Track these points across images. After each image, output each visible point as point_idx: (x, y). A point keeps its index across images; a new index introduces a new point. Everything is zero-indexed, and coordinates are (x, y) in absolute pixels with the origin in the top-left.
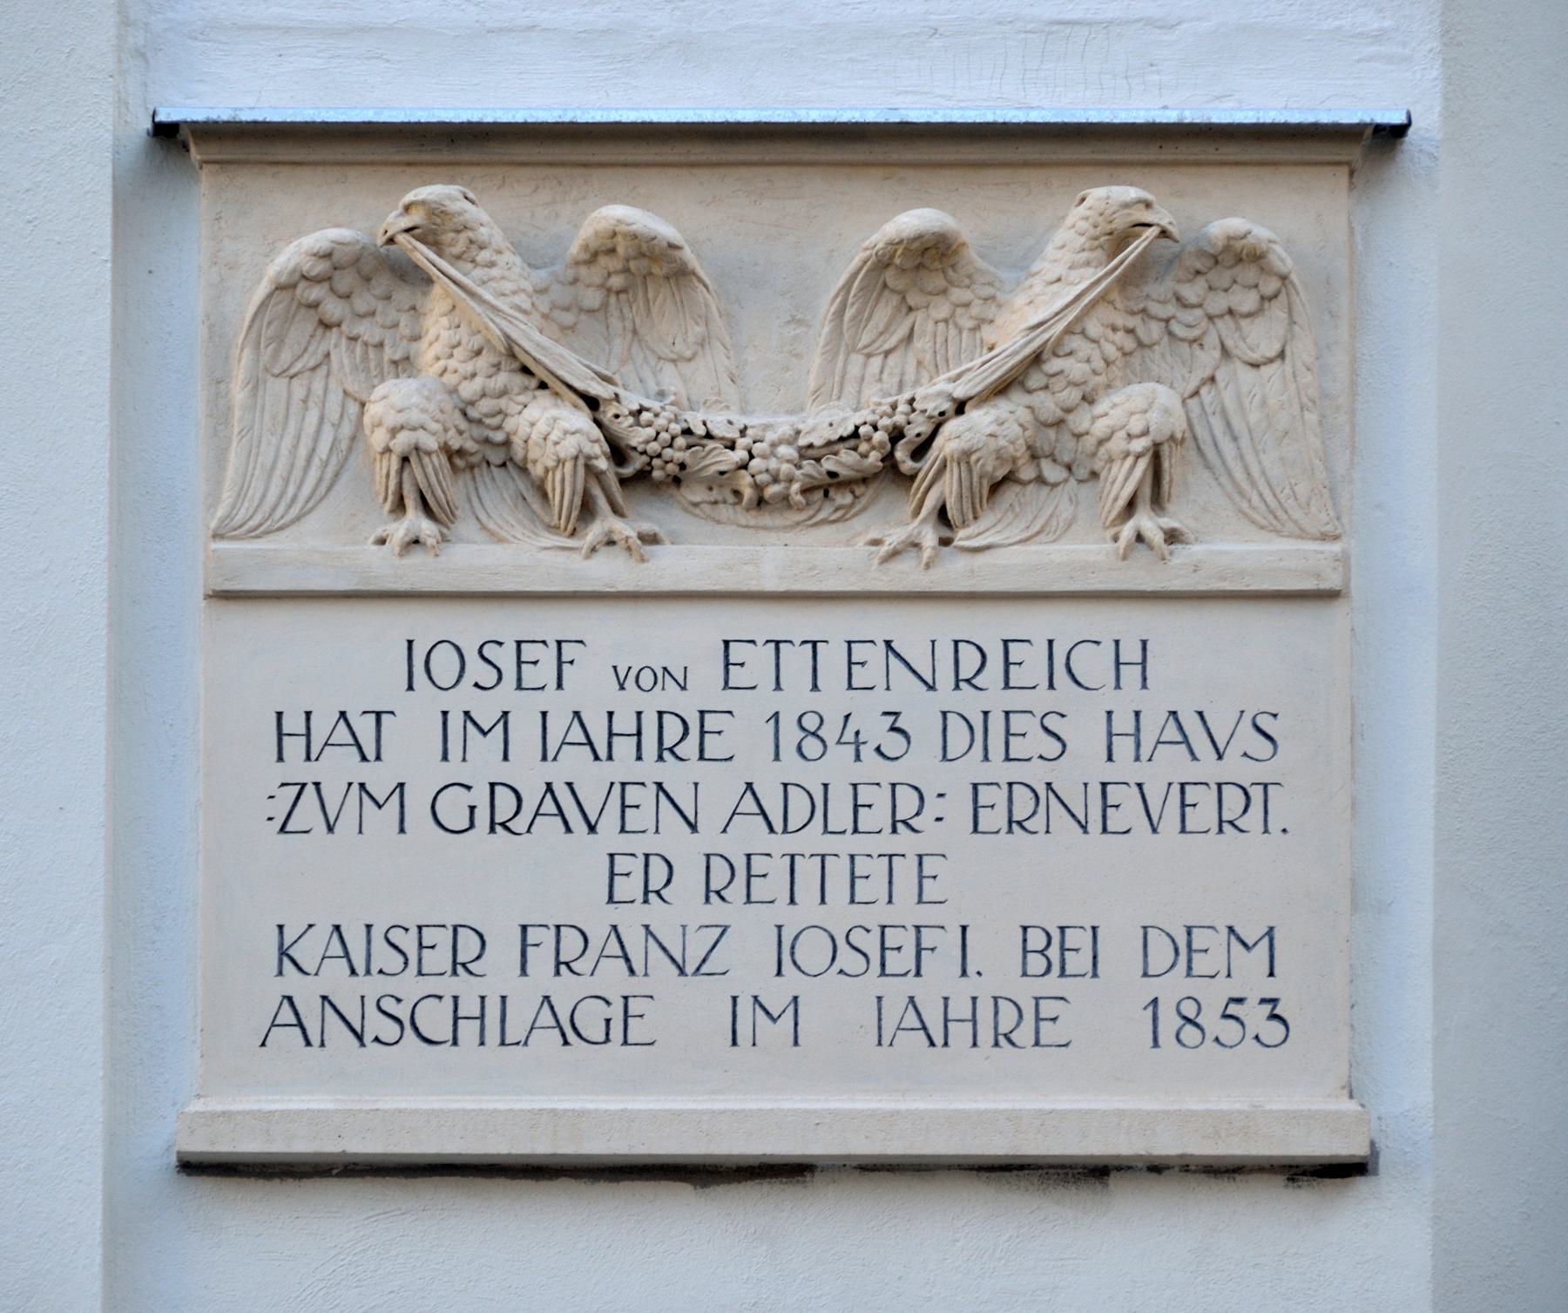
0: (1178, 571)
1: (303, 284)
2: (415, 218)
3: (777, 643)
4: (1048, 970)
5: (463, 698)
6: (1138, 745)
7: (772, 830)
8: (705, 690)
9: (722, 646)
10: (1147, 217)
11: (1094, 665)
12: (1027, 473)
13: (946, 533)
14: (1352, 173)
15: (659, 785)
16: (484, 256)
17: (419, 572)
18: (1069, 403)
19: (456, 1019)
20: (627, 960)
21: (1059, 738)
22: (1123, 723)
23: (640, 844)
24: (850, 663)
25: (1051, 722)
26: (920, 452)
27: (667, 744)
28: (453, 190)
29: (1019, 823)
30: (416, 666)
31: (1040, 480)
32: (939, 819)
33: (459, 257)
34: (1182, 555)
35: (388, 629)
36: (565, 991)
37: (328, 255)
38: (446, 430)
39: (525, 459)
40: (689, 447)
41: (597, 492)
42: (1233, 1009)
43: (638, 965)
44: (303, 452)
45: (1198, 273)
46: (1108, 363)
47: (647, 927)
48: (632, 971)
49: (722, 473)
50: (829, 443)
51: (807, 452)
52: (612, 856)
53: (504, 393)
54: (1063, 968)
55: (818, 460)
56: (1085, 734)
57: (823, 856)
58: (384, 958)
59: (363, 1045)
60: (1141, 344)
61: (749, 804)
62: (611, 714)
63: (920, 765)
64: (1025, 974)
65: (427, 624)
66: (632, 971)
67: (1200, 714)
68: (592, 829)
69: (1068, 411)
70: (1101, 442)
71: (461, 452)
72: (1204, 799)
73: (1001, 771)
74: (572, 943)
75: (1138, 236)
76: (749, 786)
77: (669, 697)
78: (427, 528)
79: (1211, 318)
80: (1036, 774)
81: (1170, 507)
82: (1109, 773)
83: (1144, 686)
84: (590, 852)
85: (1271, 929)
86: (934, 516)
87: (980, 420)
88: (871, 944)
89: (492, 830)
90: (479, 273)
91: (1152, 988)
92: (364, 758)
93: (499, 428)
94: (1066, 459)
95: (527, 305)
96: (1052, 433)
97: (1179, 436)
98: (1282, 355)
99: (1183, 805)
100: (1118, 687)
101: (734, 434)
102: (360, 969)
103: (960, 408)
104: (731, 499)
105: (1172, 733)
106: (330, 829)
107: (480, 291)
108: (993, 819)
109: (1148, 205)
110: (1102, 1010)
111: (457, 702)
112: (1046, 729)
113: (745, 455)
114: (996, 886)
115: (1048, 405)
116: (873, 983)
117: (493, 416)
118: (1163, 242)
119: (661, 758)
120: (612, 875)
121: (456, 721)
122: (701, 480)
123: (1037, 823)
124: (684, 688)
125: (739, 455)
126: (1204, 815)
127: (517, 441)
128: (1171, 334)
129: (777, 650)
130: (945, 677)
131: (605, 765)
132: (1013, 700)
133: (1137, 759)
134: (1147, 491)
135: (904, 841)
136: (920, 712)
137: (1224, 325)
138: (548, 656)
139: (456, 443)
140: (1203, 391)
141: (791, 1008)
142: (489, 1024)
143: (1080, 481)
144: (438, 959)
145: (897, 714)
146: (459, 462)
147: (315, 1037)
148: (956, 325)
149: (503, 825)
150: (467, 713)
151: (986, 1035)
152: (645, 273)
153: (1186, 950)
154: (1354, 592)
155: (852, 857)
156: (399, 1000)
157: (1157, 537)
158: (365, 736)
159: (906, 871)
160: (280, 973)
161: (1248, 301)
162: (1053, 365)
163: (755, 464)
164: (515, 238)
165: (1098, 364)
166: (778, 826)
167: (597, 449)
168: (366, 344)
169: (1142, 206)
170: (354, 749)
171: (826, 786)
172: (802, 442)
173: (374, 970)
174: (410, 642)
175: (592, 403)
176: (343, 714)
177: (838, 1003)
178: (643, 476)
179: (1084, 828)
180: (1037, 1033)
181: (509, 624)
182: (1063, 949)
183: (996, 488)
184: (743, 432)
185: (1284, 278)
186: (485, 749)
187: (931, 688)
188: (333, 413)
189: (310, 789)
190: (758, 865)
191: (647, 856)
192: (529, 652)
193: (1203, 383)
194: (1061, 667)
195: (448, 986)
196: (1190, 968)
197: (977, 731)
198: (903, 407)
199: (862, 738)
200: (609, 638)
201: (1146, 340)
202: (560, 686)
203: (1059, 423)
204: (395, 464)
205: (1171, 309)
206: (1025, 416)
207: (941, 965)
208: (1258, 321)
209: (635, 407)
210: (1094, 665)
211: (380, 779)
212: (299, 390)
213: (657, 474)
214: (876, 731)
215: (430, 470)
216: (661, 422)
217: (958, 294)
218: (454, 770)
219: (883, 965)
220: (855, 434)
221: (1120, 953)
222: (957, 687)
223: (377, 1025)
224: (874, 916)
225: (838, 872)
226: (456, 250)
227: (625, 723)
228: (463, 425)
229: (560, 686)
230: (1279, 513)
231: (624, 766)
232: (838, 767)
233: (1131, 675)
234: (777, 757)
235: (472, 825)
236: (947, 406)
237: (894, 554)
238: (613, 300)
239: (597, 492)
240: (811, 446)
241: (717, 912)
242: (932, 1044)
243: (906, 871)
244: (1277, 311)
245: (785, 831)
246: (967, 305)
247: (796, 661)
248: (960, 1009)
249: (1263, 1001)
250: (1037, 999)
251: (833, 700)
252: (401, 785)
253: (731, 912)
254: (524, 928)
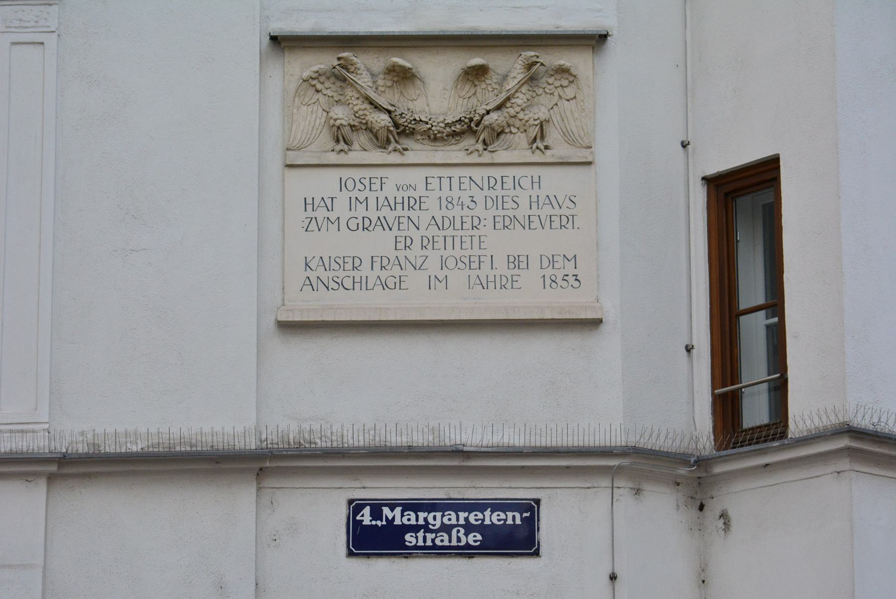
0: (549, 157)
5: (355, 193)
8: (421, 190)
10: (538, 60)
11: (526, 183)
12: (507, 130)
16: (359, 72)
22: (534, 199)
23: (404, 234)
26: (477, 125)
28: (351, 54)
30: (343, 185)
31: (511, 132)
36: (384, 275)
37: (317, 72)
41: (391, 137)
42: (565, 278)
43: (403, 267)
51: (447, 125)
56: (524, 202)
58: (334, 266)
61: (433, 222)
63: (479, 211)
65: (346, 173)
71: (354, 126)
73: (501, 212)
77: (411, 193)
78: (346, 147)
80: (511, 213)
84: (390, 236)
87: (494, 116)
88: (467, 261)
91: (543, 272)
98: (575, 97)
103: (488, 112)
105: (547, 201)
109: (538, 57)
110: (530, 278)
111: (354, 194)
114: (500, 244)
115: (512, 111)
116: (467, 272)
121: (353, 200)
123: (511, 227)
126: (557, 224)
130: (486, 187)
132: (504, 193)
134: (539, 135)
136: (479, 196)
137: (560, 89)
142: (363, 284)
144: (349, 266)
151: (498, 286)
153: (552, 262)
154: (596, 161)
157: (542, 148)
158: (329, 204)
162: (513, 101)
164: (368, 66)
175: (389, 112)
177: (458, 278)
178: (404, 132)
181: (367, 173)
183: (499, 134)
185: (575, 76)
188: (319, 115)
192: (373, 181)
195: (351, 273)
197: (495, 201)
200: (395, 176)
203: (515, 117)
207: (486, 266)
210: (526, 183)
212: (310, 109)
214: (467, 202)
218: (353, 213)
220: (460, 120)
221: (534, 262)
223: (332, 285)
227: (399, 200)
231: (399, 211)
232: (457, 212)
233: (536, 185)
239: (391, 137)
241: (425, 252)
247: (445, 182)
248: (491, 278)
251: (456, 193)
253: (429, 252)
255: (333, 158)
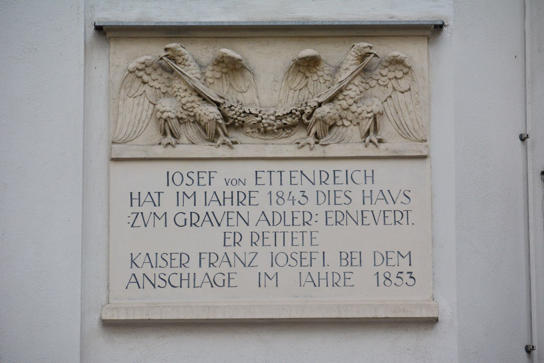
1: (137, 71)
2: (169, 53)
3: (271, 172)
4: (347, 264)
5: (183, 188)
6: (372, 200)
7: (269, 225)
8: (251, 185)
9: (255, 173)
10: (371, 51)
11: (359, 177)
12: (340, 123)
13: (317, 140)
14: (428, 39)
15: (238, 212)
16: (187, 63)
17: (170, 152)
18: (350, 104)
19: (181, 280)
20: (229, 262)
21: (349, 198)
22: (367, 194)
23: (233, 229)
24: (291, 177)
25: (348, 194)
26: (309, 117)
27: (240, 201)
28: (178, 45)
29: (339, 222)
30: (170, 179)
31: (343, 125)
32: (316, 221)
33: (180, 64)
34: (382, 146)
35: (163, 168)
36: (212, 272)
37: (144, 63)
38: (177, 112)
39: (199, 120)
40: (245, 116)
41: (219, 130)
42: (400, 275)
43: (232, 264)
44: (138, 118)
45: (386, 67)
46: (361, 92)
47: (235, 253)
48: (231, 266)
49: (254, 124)
50: (284, 115)
51: (278, 118)
52: (225, 233)
53: (193, 102)
54: (352, 264)
55: (281, 120)
56: (357, 197)
57: (284, 232)
58: (161, 263)
59: (155, 288)
60: (370, 87)
61: (263, 218)
62: (224, 192)
63: (311, 206)
64: (341, 266)
65: (172, 167)
66: (231, 266)
67: (389, 191)
68: (219, 225)
69: (350, 105)
70: (360, 114)
71: (182, 118)
72: (390, 215)
74: (214, 258)
75: (369, 56)
76: (263, 212)
77: (240, 188)
78: (173, 140)
79: (390, 79)
80: (343, 208)
81: (379, 133)
82: (364, 208)
83: (373, 183)
84: (218, 232)
85: (410, 252)
86: (313, 136)
87: (326, 109)
88: (298, 257)
89: (191, 226)
90: (187, 68)
92: (155, 205)
93: (192, 111)
94: (350, 119)
95: (199, 77)
96: (346, 112)
97: (381, 112)
98: (409, 89)
99: (384, 217)
100: (366, 183)
101: (257, 113)
102: (154, 266)
103: (320, 105)
104: (257, 131)
105: (381, 196)
106: (146, 226)
107: (186, 73)
108: (331, 221)
109: (371, 48)
110: (363, 275)
111: (181, 189)
112: (346, 195)
113: (260, 119)
114: (333, 240)
115: (344, 104)
116: (298, 268)
117: (190, 108)
118: (376, 58)
119: (238, 204)
120: (225, 238)
121: (181, 195)
122: (249, 126)
123: (344, 222)
124: (245, 185)
125: (259, 119)
127: (197, 115)
128: (379, 84)
129: (271, 173)
130: (317, 181)
131: (223, 207)
132: (337, 187)
133: (371, 204)
135: (306, 228)
136: (311, 191)
137: (394, 81)
138: (206, 176)
139: (180, 116)
140: (388, 100)
141: (275, 276)
142: (190, 281)
143: (354, 125)
144: (176, 263)
145: (304, 192)
146: (181, 121)
147: (141, 286)
148: (320, 82)
149: (194, 224)
150: (184, 192)
151: (330, 283)
152: (232, 68)
153: (386, 258)
155: (292, 232)
156: (165, 275)
157: (376, 141)
158: (156, 199)
159: (307, 236)
160: (132, 267)
161: (399, 74)
162: (346, 93)
163: (264, 121)
164: (197, 56)
165: (358, 92)
166: (271, 224)
167: (219, 117)
168: (156, 88)
169: (369, 48)
170: (152, 203)
171: (284, 212)
172: (277, 115)
173: (158, 266)
174: (168, 172)
175: (218, 104)
176: (149, 193)
177: (289, 275)
178: (233, 124)
179: (357, 224)
180: (345, 282)
182: (351, 258)
183: (331, 127)
184: (260, 112)
185: (409, 68)
186: (189, 203)
187: (314, 184)
189: (140, 214)
190: (266, 235)
191: (235, 233)
192: (201, 175)
193: (388, 97)
194: (349, 178)
195: (179, 270)
196: (387, 263)
198: (304, 105)
199: (294, 199)
200: (224, 170)
201: (372, 86)
202: (210, 184)
203: (347, 109)
204: (163, 121)
205: (379, 77)
206: (339, 107)
208: (403, 80)
209: (230, 105)
210: (359, 177)
211: (160, 211)
212: (136, 101)
213: (237, 124)
214: (298, 197)
215: (173, 123)
216: (237, 109)
217: (320, 73)
218: (180, 209)
219: (301, 263)
220: (291, 112)
221: (368, 259)
222: (321, 184)
223: (159, 282)
224: (298, 249)
225: (288, 236)
226: (179, 62)
227: (228, 195)
228: (182, 111)
229: (210, 184)
230: (410, 135)
231: (228, 206)
232: (288, 207)
233: (369, 180)
234: (271, 204)
235: (185, 224)
236: (316, 104)
237: (303, 146)
238: (224, 75)
240: (279, 116)
241: (254, 249)
242: (315, 286)
243: (307, 236)
244: (407, 77)
245: (273, 225)
246: (322, 76)
247: (276, 177)
248: (323, 276)
249: (408, 273)
250: (344, 273)
251: (286, 188)
252: (166, 213)
253: (258, 248)
254: (200, 254)
255: (160, 152)
